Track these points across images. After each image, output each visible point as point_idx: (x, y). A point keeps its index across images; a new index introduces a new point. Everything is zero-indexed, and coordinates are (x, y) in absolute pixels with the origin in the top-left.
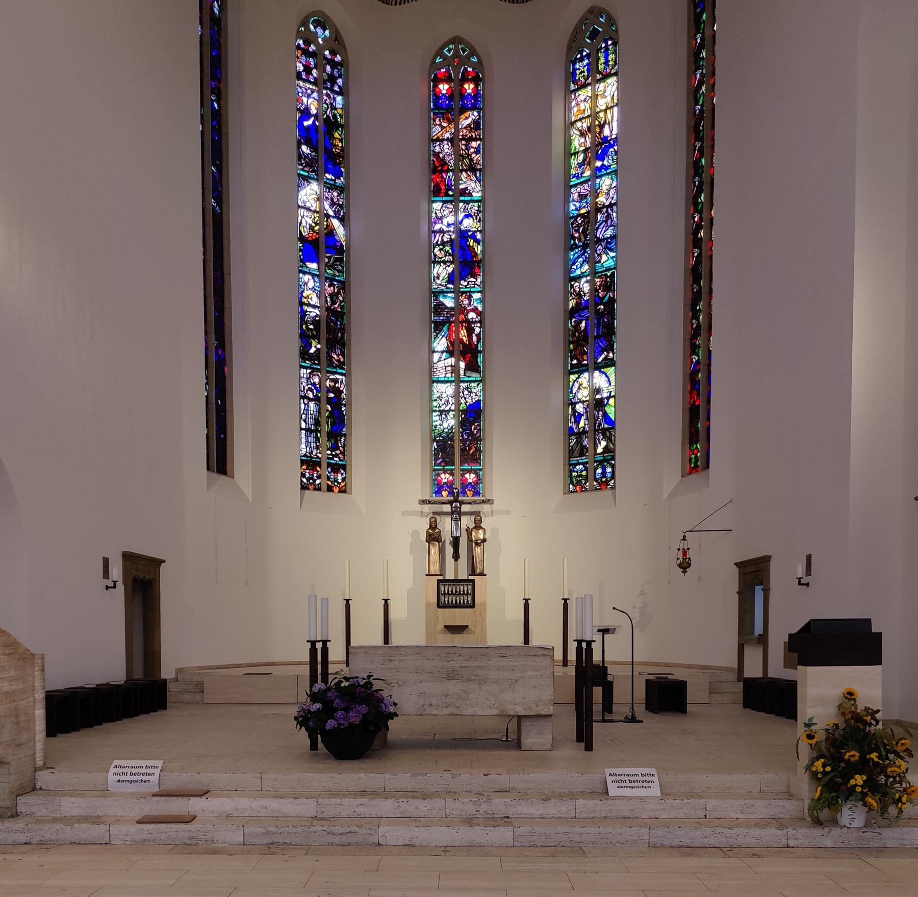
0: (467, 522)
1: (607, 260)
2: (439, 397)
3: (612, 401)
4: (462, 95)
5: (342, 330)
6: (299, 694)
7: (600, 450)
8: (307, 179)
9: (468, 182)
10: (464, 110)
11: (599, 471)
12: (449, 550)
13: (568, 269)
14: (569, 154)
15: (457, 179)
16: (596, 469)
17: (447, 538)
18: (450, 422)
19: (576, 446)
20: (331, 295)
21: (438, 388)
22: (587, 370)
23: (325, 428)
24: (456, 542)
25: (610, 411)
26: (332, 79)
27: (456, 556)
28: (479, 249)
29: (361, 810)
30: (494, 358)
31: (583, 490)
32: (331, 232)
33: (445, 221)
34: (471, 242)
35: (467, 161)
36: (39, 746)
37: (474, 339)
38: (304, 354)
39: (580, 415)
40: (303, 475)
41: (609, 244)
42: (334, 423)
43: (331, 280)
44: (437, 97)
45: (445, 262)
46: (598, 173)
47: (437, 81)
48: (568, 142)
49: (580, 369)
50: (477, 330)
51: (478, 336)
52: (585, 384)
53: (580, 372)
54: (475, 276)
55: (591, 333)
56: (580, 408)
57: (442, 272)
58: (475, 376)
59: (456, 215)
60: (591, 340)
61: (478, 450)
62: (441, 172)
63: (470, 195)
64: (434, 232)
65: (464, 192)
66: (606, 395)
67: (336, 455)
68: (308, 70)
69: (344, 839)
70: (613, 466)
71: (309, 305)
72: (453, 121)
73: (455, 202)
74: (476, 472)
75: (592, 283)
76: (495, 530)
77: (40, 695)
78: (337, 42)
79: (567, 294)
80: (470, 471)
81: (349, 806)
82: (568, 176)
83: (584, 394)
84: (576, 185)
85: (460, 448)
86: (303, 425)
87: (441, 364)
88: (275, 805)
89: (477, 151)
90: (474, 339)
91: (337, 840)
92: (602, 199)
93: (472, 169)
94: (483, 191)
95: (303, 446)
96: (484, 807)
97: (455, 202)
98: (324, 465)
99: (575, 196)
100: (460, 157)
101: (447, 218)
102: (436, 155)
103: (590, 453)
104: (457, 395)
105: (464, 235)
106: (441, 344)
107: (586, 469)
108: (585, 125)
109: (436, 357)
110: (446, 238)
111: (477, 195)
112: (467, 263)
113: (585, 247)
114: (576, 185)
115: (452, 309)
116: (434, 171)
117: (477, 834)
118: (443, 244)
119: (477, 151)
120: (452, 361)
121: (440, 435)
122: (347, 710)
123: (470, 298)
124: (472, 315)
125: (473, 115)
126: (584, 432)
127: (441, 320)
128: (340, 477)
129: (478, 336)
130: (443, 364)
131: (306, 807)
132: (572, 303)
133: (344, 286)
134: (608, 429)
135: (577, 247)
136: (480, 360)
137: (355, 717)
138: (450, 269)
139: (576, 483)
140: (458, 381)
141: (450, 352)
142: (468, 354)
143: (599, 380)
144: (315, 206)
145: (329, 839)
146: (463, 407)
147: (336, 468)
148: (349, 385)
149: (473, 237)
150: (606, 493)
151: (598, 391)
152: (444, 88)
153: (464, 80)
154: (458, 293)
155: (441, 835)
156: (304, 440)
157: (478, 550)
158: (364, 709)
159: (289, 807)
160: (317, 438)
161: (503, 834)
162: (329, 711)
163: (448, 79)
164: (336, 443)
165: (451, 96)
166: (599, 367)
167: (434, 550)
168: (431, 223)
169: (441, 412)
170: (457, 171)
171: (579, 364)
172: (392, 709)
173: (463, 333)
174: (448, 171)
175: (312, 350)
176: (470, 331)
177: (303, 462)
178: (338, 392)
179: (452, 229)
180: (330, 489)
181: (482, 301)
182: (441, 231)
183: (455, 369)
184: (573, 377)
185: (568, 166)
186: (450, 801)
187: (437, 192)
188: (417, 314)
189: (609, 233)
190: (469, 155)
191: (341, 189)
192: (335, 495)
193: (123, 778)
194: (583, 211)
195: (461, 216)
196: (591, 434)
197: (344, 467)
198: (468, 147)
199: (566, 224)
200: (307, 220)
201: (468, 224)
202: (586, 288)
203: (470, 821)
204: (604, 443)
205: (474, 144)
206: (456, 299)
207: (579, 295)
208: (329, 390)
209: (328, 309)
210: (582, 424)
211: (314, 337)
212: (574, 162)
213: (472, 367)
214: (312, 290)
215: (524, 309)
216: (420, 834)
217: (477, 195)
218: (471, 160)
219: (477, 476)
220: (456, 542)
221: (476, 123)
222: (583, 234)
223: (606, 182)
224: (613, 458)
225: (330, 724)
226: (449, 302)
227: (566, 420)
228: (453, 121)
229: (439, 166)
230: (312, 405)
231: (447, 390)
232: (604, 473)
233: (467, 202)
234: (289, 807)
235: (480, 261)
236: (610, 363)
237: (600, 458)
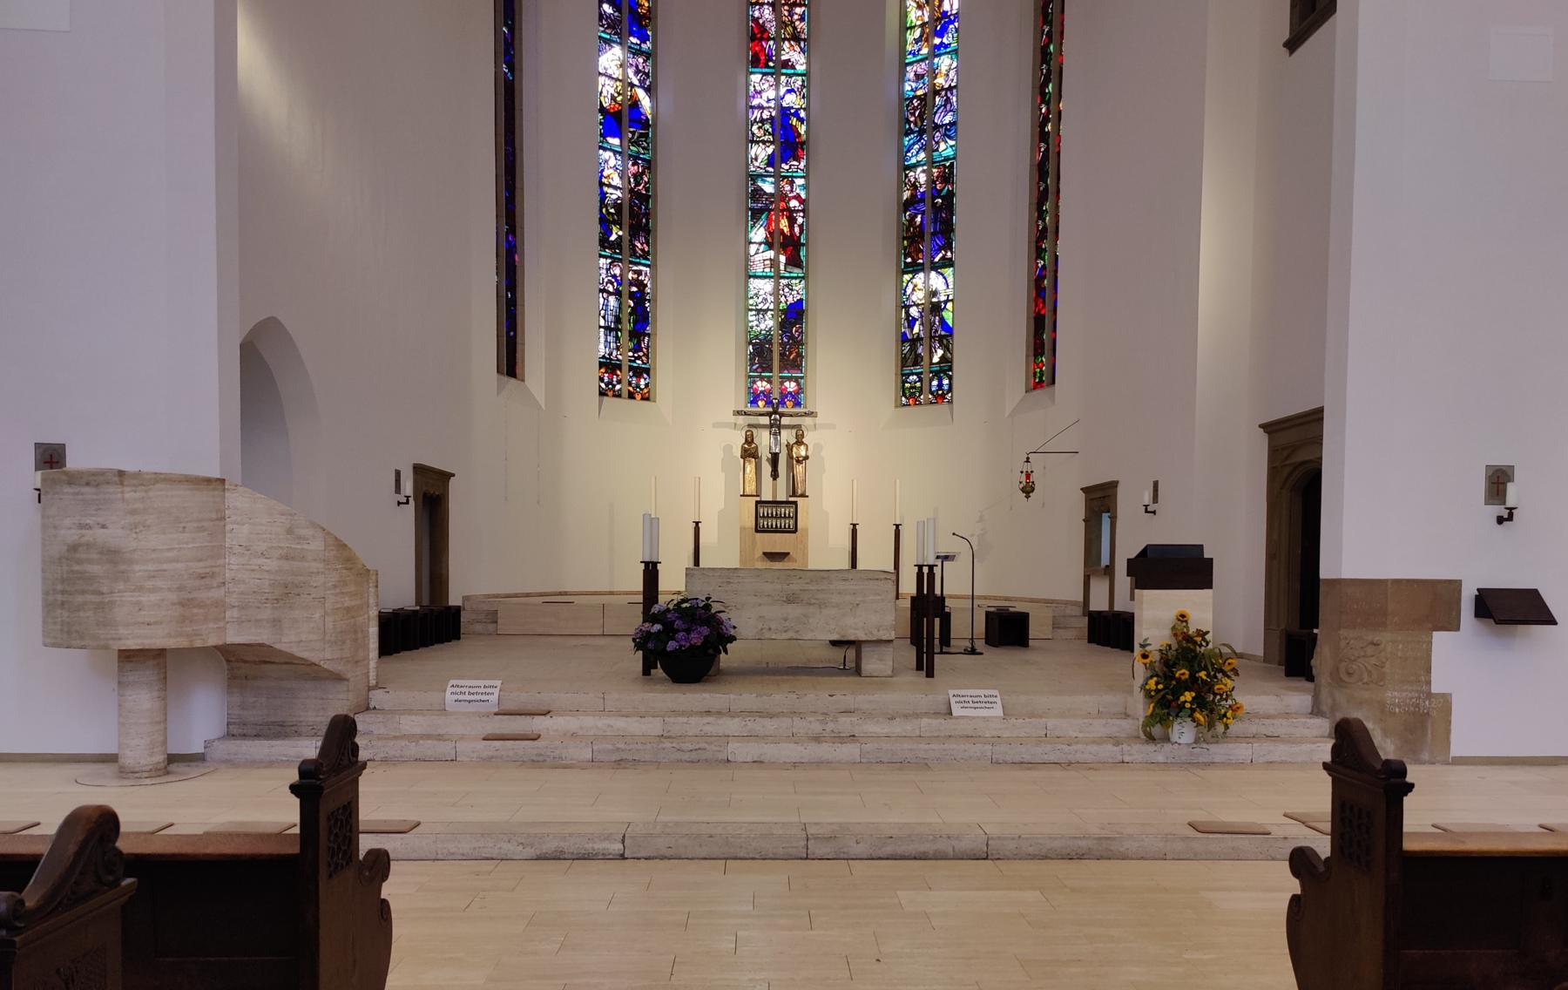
0: (787, 436)
1: (945, 148)
2: (756, 295)
3: (949, 306)
5: (647, 215)
6: (634, 621)
7: (936, 359)
9: (791, 53)
11: (935, 383)
12: (767, 469)
13: (902, 157)
14: (905, 28)
15: (779, 49)
16: (931, 380)
17: (765, 454)
18: (769, 323)
19: (909, 354)
20: (635, 176)
21: (755, 284)
22: (922, 270)
23: (627, 326)
24: (774, 459)
25: (948, 316)
27: (775, 475)
28: (802, 129)
29: (708, 729)
31: (917, 403)
33: (765, 95)
34: (794, 121)
35: (790, 29)
36: (372, 664)
37: (797, 230)
39: (915, 320)
40: (601, 379)
41: (949, 131)
42: (636, 320)
43: (635, 159)
45: (764, 142)
46: (937, 51)
48: (904, 14)
49: (914, 268)
50: (800, 220)
51: (801, 226)
52: (920, 286)
53: (915, 272)
54: (798, 159)
55: (927, 229)
56: (914, 312)
57: (761, 152)
58: (797, 272)
59: (777, 89)
60: (927, 237)
61: (800, 355)
62: (761, 39)
63: (793, 67)
64: (753, 108)
66: (943, 298)
67: (639, 358)
69: (694, 756)
70: (950, 378)
71: (609, 186)
73: (776, 74)
74: (796, 380)
75: (928, 173)
76: (818, 447)
77: (374, 613)
79: (902, 182)
80: (790, 379)
81: (696, 725)
82: (903, 52)
83: (918, 296)
84: (911, 63)
85: (780, 351)
86: (602, 323)
87: (759, 257)
88: (620, 724)
89: (802, 19)
90: (797, 230)
91: (686, 757)
92: (940, 81)
93: (795, 37)
94: (808, 63)
95: (602, 346)
96: (830, 726)
97: (776, 74)
98: (625, 368)
99: (911, 75)
100: (782, 24)
101: (766, 92)
102: (756, 20)
103: (925, 362)
104: (776, 293)
105: (785, 113)
106: (759, 234)
107: (921, 380)
109: (753, 249)
110: (766, 115)
111: (801, 68)
112: (789, 145)
113: (921, 132)
114: (911, 63)
115: (772, 195)
116: (753, 38)
117: (825, 751)
118: (762, 121)
119: (802, 19)
120: (771, 254)
121: (756, 337)
122: (688, 631)
123: (792, 183)
124: (794, 203)
126: (919, 339)
127: (759, 207)
128: (642, 382)
129: (801, 226)
130: (761, 257)
131: (653, 726)
132: (907, 195)
133: (649, 165)
134: (944, 336)
135: (912, 132)
136: (803, 253)
137: (696, 639)
138: (770, 150)
139: (909, 395)
140: (778, 277)
141: (769, 244)
142: (790, 246)
143: (936, 281)
145: (678, 756)
146: (783, 306)
147: (638, 372)
148: (654, 278)
149: (796, 115)
150: (943, 408)
151: (935, 293)
155: (789, 752)
156: (602, 340)
157: (799, 469)
158: (705, 631)
159: (633, 726)
160: (617, 338)
161: (849, 751)
162: (669, 631)
164: (639, 344)
166: (935, 267)
167: (750, 468)
168: (748, 97)
169: (759, 311)
170: (779, 40)
171: (914, 263)
172: (732, 632)
173: (784, 224)
174: (769, 39)
175: (613, 238)
176: (792, 221)
177: (601, 365)
178: (641, 285)
179: (772, 104)
180: (631, 396)
181: (806, 187)
182: (760, 107)
183: (774, 263)
184: (907, 277)
185: (903, 42)
186: (797, 720)
187: (758, 61)
188: (734, 201)
189: (948, 119)
190: (792, 22)
192: (637, 403)
193: (461, 697)
194: (920, 93)
195: (783, 90)
196: (926, 342)
197: (647, 371)
198: (791, 14)
199: (901, 105)
201: (791, 100)
202: (923, 178)
203: (817, 739)
204: (940, 352)
205: (798, 10)
206: (776, 184)
207: (914, 186)
208: (631, 283)
209: (631, 191)
210: (916, 330)
211: (615, 223)
212: (910, 37)
213: (794, 261)
215: (853, 197)
216: (769, 751)
217: (801, 68)
218: (795, 28)
219: (798, 384)
220: (774, 459)
222: (919, 118)
224: (951, 369)
225: (672, 645)
226: (768, 187)
227: (899, 325)
229: (758, 33)
231: (766, 286)
232: (940, 385)
233: (790, 76)
234: (633, 726)
235: (803, 143)
237: (936, 368)
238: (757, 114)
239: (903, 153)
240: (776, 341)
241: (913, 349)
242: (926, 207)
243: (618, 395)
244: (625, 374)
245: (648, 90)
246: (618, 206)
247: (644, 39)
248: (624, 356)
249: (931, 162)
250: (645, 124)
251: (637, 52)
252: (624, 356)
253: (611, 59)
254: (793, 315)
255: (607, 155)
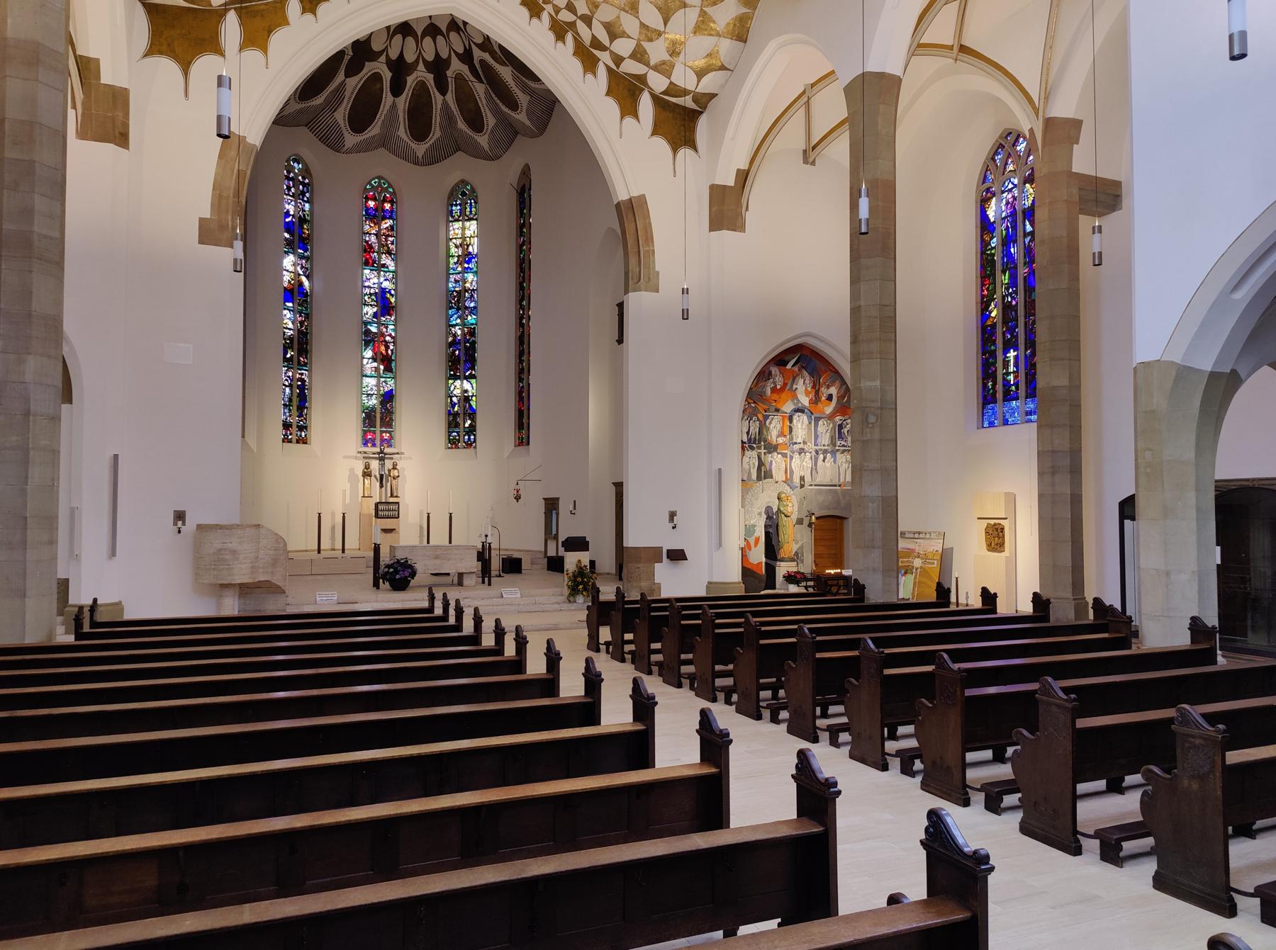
1: (471, 319)
4: (383, 210)
8: (286, 253)
9: (386, 260)
10: (384, 218)
13: (448, 320)
14: (449, 256)
15: (380, 258)
18: (374, 401)
19: (452, 422)
21: (366, 380)
25: (473, 404)
26: (303, 193)
28: (393, 300)
30: (401, 365)
31: (457, 447)
32: (301, 284)
38: (285, 359)
41: (473, 311)
42: (300, 400)
43: (300, 313)
44: (367, 209)
46: (466, 270)
47: (367, 199)
48: (448, 249)
49: (455, 378)
55: (461, 358)
56: (455, 399)
57: (370, 311)
58: (389, 375)
61: (391, 420)
65: (384, 266)
68: (289, 188)
72: (378, 224)
73: (379, 271)
78: (306, 172)
79: (448, 333)
83: (457, 392)
85: (379, 419)
92: (468, 285)
93: (389, 253)
97: (379, 271)
100: (381, 245)
101: (372, 280)
104: (378, 385)
105: (383, 291)
106: (369, 353)
108: (458, 242)
109: (365, 361)
111: (392, 268)
112: (385, 306)
113: (458, 309)
116: (365, 251)
120: (375, 364)
124: (388, 338)
125: (388, 223)
127: (369, 339)
130: (369, 366)
133: (308, 317)
134: (472, 414)
139: (453, 443)
140: (379, 377)
141: (374, 359)
142: (386, 361)
143: (467, 385)
144: (292, 269)
148: (310, 377)
150: (471, 450)
151: (466, 391)
152: (371, 204)
153: (385, 200)
154: (379, 324)
163: (374, 199)
165: (376, 209)
166: (466, 378)
170: (379, 253)
173: (383, 348)
176: (387, 348)
178: (303, 381)
181: (394, 330)
183: (377, 369)
185: (448, 263)
187: (366, 263)
189: (472, 305)
191: (307, 259)
192: (301, 446)
200: (287, 277)
201: (386, 284)
202: (459, 332)
206: (378, 328)
207: (455, 335)
213: (388, 369)
214: (288, 319)
221: (392, 227)
222: (457, 301)
223: (470, 277)
226: (374, 329)
228: (378, 224)
229: (368, 248)
230: (288, 390)
231: (373, 382)
236: (473, 377)
238: (367, 291)
239: (448, 318)
240: (378, 411)
241: (455, 419)
242: (462, 347)
243: (290, 441)
244: (294, 429)
245: (307, 277)
246: (291, 338)
247: (306, 250)
248: (294, 420)
249: (464, 325)
250: (306, 295)
251: (302, 257)
252: (294, 420)
253: (289, 261)
254: (388, 397)
255: (285, 312)
